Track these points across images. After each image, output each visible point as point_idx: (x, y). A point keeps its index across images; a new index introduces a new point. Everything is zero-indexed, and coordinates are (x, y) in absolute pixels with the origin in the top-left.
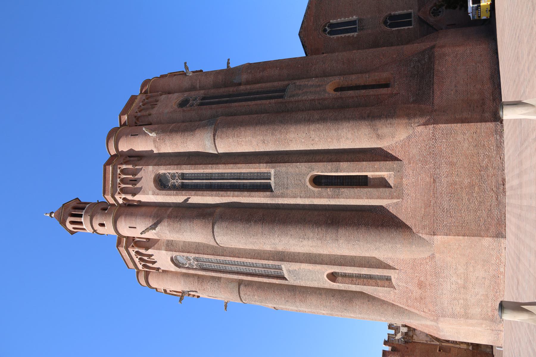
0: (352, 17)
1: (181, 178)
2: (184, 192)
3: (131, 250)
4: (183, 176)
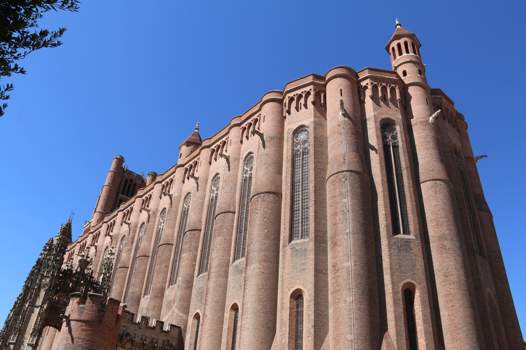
1: (393, 144)
2: (381, 146)
3: (311, 87)
4: (396, 147)
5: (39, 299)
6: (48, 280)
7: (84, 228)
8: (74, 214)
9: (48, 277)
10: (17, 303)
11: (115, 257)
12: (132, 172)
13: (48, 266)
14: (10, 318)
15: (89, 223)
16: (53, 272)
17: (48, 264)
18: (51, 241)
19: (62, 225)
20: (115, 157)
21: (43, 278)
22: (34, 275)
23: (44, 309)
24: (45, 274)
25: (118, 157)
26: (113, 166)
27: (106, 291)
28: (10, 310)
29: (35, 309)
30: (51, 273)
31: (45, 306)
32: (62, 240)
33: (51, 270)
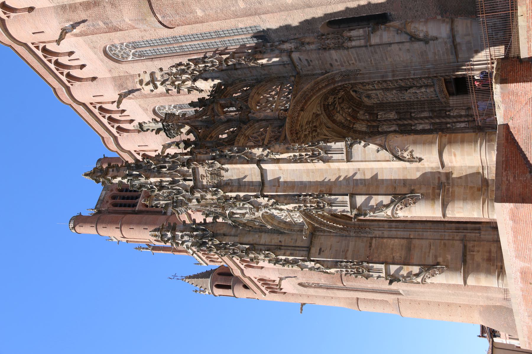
5: (245, 177)
6: (202, 170)
7: (207, 264)
8: (175, 276)
9: (195, 172)
10: (285, 260)
11: (153, 66)
12: (99, 200)
13: (173, 182)
14: (318, 265)
15: (194, 254)
16: (183, 165)
17: (170, 184)
18: (157, 233)
19: (196, 291)
20: (73, 231)
21: (199, 184)
22: (226, 244)
23: (263, 150)
24: (191, 183)
25: (72, 225)
26: (88, 230)
27: (224, 57)
28: (302, 269)
29: (270, 177)
30: (186, 168)
31: (258, 152)
32: (118, 174)
33: (179, 172)
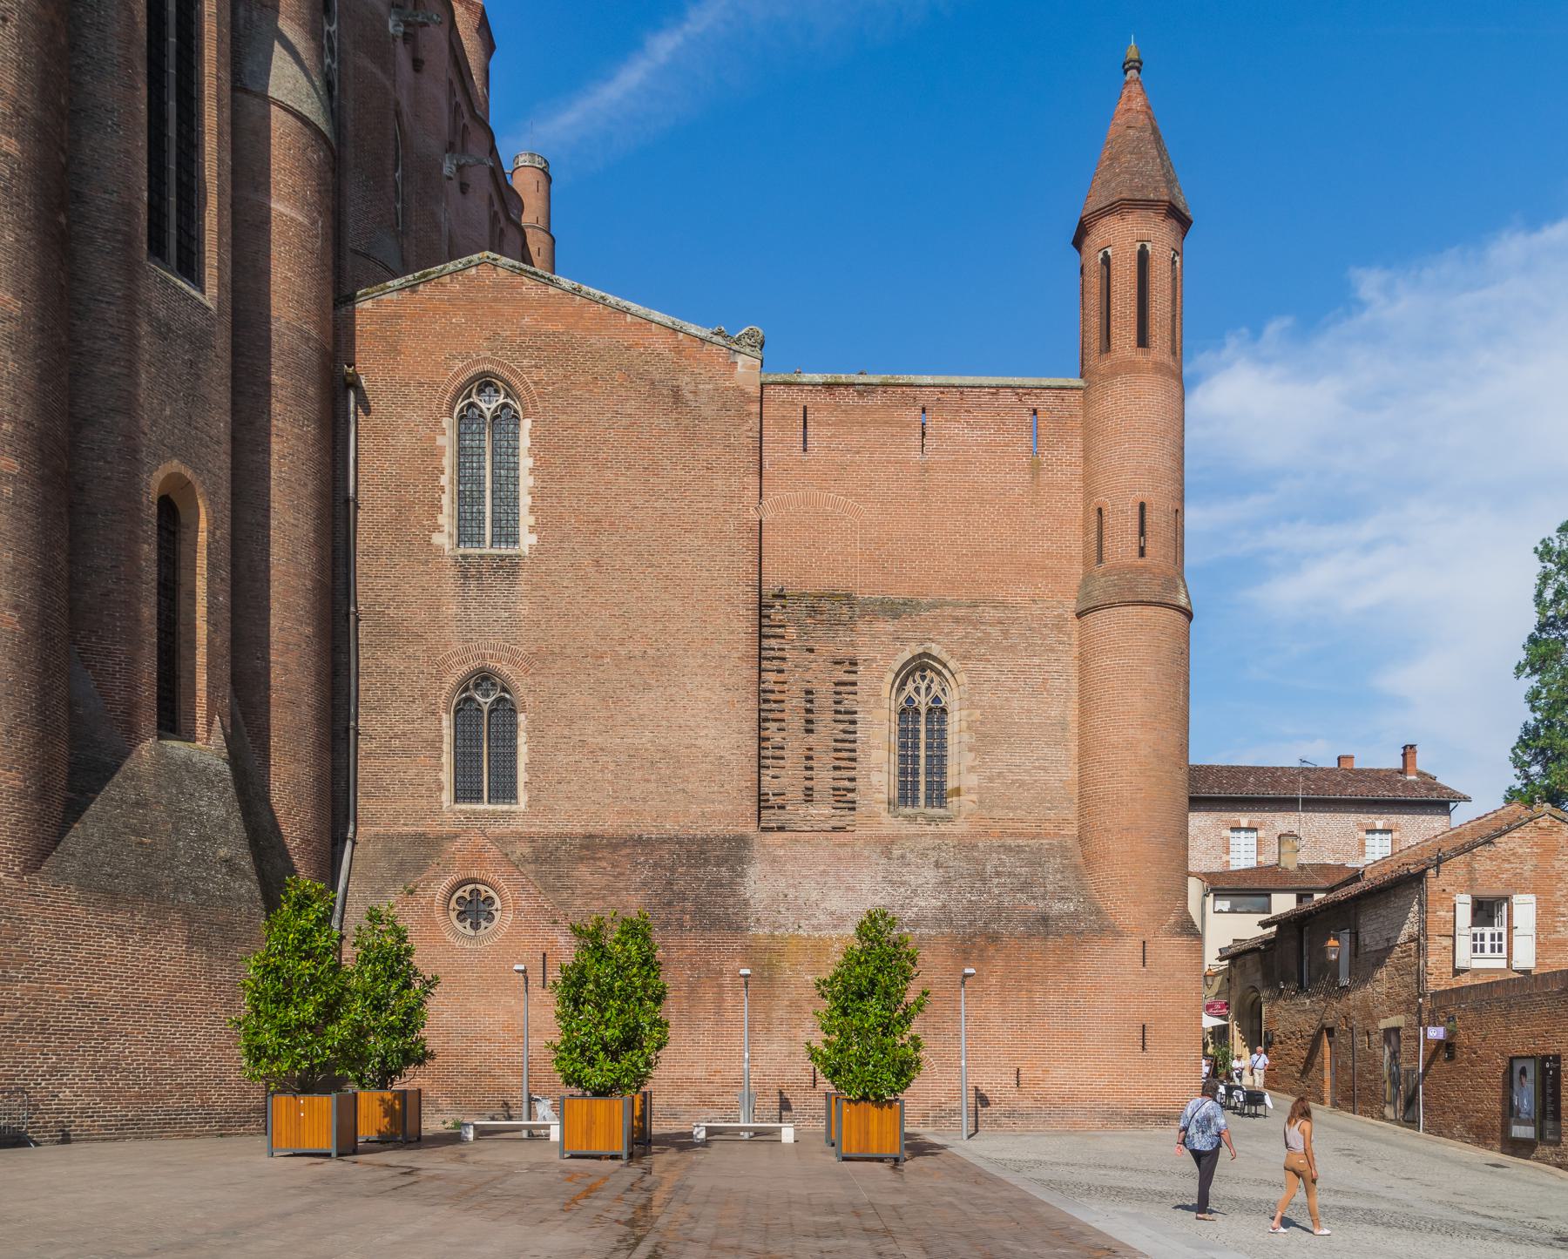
0: (532, 529)
